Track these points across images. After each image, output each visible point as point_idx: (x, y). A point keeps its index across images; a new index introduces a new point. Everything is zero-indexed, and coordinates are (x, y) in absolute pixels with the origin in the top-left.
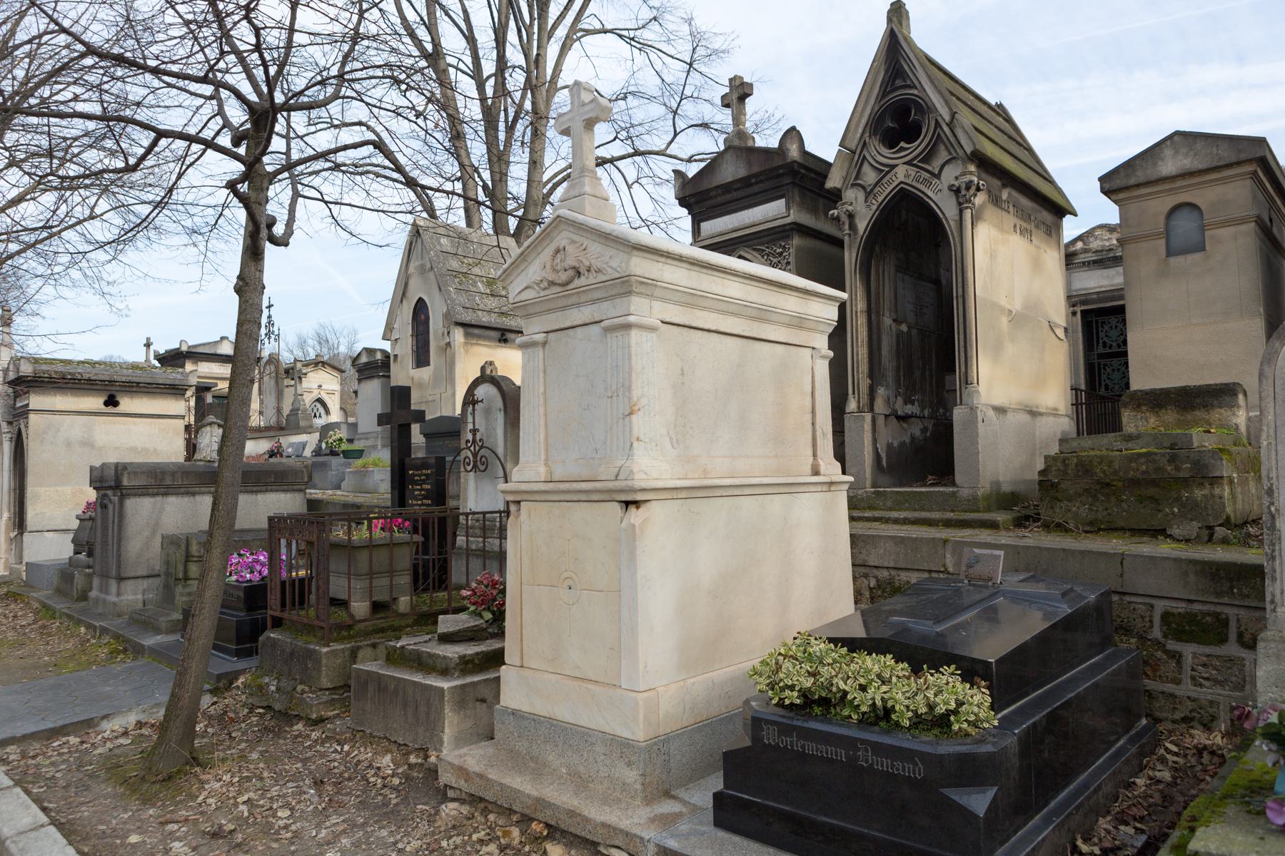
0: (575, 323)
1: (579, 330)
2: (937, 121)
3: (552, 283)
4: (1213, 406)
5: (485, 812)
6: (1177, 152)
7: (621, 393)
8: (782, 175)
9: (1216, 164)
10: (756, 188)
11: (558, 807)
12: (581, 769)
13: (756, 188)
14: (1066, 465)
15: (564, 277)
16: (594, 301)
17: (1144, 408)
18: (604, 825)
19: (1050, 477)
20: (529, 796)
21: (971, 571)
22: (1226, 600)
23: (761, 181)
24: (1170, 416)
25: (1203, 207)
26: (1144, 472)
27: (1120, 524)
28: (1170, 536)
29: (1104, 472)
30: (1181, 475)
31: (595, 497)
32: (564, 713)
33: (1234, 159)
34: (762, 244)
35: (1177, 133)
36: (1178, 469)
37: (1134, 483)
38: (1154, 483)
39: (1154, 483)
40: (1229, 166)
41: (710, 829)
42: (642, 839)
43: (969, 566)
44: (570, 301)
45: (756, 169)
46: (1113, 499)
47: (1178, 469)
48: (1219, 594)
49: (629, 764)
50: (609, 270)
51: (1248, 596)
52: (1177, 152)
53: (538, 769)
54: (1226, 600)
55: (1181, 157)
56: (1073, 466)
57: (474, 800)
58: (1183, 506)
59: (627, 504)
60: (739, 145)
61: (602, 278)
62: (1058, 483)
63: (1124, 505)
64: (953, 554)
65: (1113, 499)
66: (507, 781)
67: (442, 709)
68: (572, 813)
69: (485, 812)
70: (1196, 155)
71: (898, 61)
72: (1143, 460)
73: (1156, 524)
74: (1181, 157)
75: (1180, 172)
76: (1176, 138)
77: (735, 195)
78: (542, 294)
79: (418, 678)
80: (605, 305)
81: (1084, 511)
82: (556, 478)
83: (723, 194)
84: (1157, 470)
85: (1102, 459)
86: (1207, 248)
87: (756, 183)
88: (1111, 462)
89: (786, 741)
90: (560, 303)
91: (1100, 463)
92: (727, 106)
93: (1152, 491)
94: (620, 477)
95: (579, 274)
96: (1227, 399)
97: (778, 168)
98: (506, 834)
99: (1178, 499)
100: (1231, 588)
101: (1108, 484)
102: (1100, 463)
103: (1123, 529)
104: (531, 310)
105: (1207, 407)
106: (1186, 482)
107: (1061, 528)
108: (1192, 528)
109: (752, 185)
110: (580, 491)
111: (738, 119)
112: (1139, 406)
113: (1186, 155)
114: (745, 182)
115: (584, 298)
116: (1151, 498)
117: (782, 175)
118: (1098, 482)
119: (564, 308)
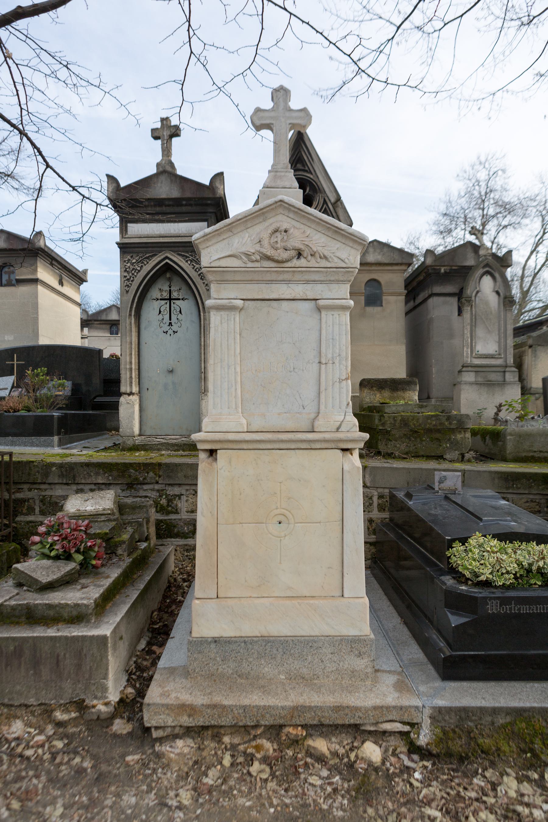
0: (283, 297)
1: (285, 304)
2: (325, 200)
3: (269, 258)
4: (406, 390)
5: (217, 737)
6: (375, 251)
7: (337, 361)
8: (207, 205)
9: (392, 262)
10: (184, 209)
11: (321, 708)
12: (305, 671)
13: (184, 209)
14: (395, 421)
15: (285, 255)
16: (307, 282)
17: (374, 388)
18: (375, 708)
19: (386, 427)
20: (283, 708)
21: (442, 485)
22: (510, 491)
23: (191, 205)
24: (387, 393)
25: (383, 283)
26: (434, 425)
27: (422, 453)
28: (445, 459)
29: (414, 425)
30: (452, 427)
31: (318, 446)
32: (279, 628)
33: (400, 262)
34: (187, 252)
35: (375, 241)
36: (450, 424)
37: (429, 431)
38: (438, 431)
39: (438, 431)
40: (397, 264)
41: (439, 683)
42: (417, 707)
43: (440, 482)
44: (281, 277)
45: (188, 195)
46: (418, 440)
47: (450, 424)
48: (507, 488)
49: (360, 655)
50: (336, 260)
51: (520, 488)
52: (375, 251)
53: (255, 682)
54: (510, 491)
55: (377, 254)
56: (398, 421)
57: (189, 732)
58: (452, 443)
59: (344, 450)
60: (166, 170)
61: (324, 263)
62: (390, 431)
63: (424, 443)
64: (370, 475)
65: (418, 440)
66: (246, 702)
67: (107, 656)
68: (338, 709)
69: (217, 737)
70: (383, 254)
71: (300, 152)
72: (434, 419)
73: (439, 453)
74: (377, 254)
75: (376, 262)
76: (375, 243)
77: (164, 209)
78: (250, 265)
79: (51, 632)
80: (319, 287)
81: (403, 447)
82: (254, 428)
83: (155, 206)
84: (441, 424)
85: (414, 417)
86: (384, 304)
87: (186, 205)
88: (418, 419)
89: (506, 609)
90: (268, 277)
91: (413, 420)
92: (156, 138)
93: (438, 435)
94: (343, 429)
95: (299, 255)
96: (413, 386)
97: (209, 199)
98: (258, 748)
99: (449, 440)
100: (513, 485)
101: (416, 432)
102: (413, 420)
103: (423, 456)
104: (229, 277)
105: (404, 390)
106: (453, 431)
107: (389, 455)
108: (455, 454)
109: (182, 205)
110: (282, 441)
111: (167, 151)
112: (372, 387)
113: (379, 254)
114: (177, 202)
115: (298, 277)
116: (437, 439)
117: (207, 205)
118: (411, 430)
119: (271, 282)
